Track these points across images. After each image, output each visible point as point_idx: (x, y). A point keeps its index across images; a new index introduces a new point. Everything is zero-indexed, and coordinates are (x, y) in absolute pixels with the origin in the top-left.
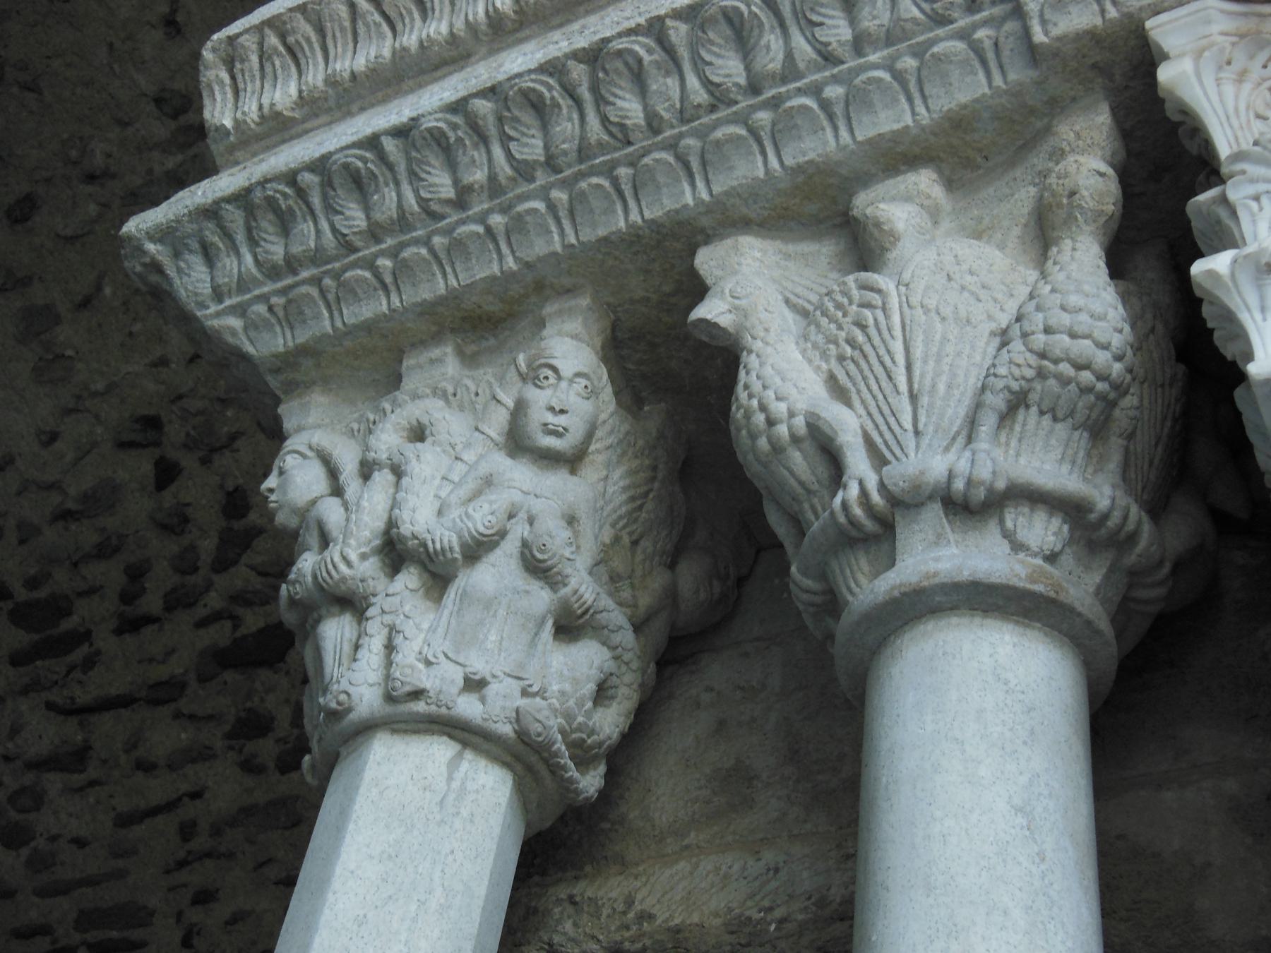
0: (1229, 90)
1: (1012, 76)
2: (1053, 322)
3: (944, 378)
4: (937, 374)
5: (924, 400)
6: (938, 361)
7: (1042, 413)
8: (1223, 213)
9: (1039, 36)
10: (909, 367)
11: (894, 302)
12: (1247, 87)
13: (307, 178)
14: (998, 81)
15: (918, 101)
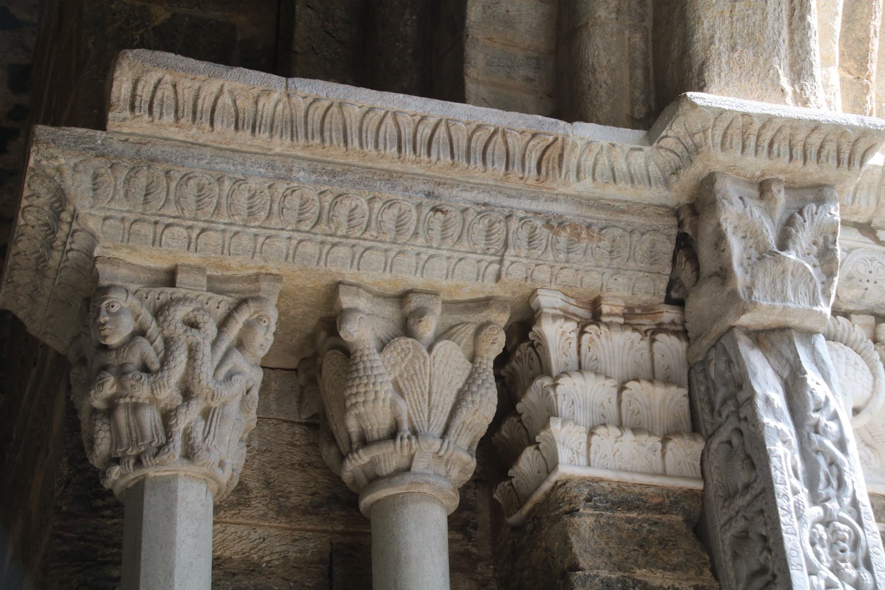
4: (439, 402)
5: (434, 411)
6: (441, 396)
8: (552, 394)
9: (503, 276)
10: (430, 394)
11: (428, 363)
13: (176, 175)
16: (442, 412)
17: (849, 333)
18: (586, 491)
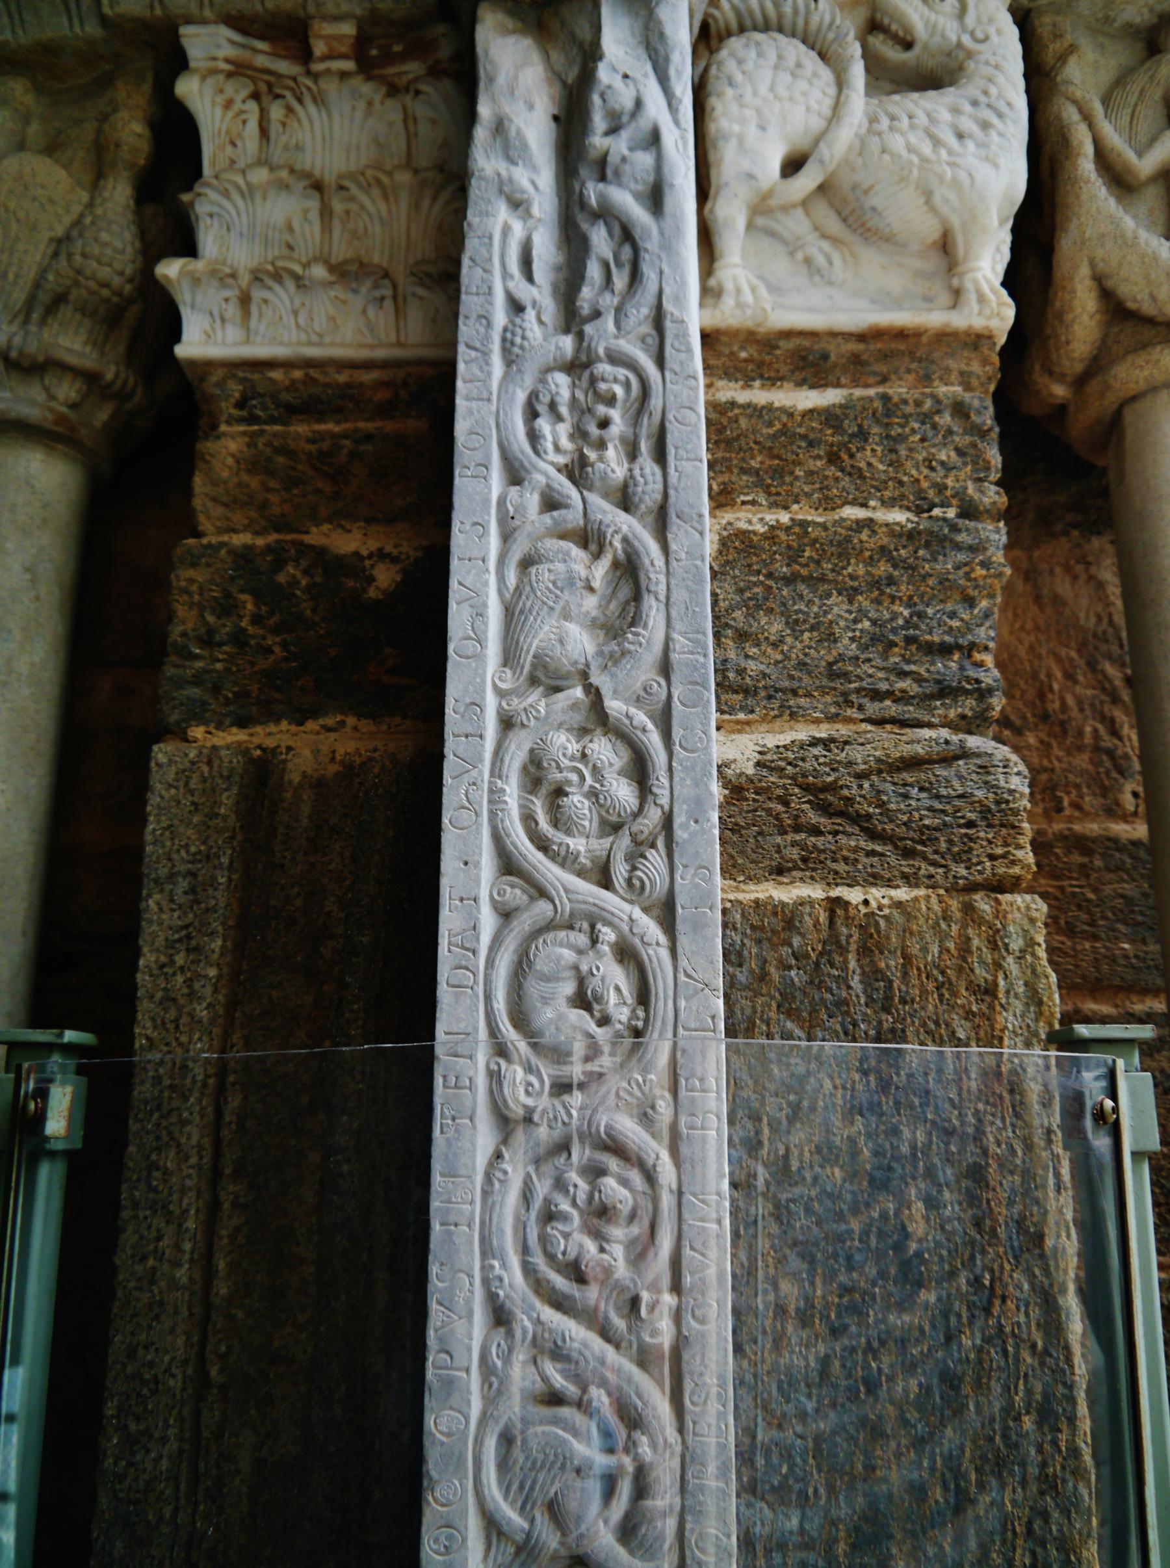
0: (219, 111)
1: (88, 29)
2: (87, 249)
3: (14, 269)
7: (76, 309)
12: (230, 114)
14: (77, 29)
15: (17, 22)
16: (15, 283)
17: (808, 12)
18: (235, 389)
